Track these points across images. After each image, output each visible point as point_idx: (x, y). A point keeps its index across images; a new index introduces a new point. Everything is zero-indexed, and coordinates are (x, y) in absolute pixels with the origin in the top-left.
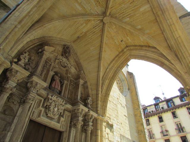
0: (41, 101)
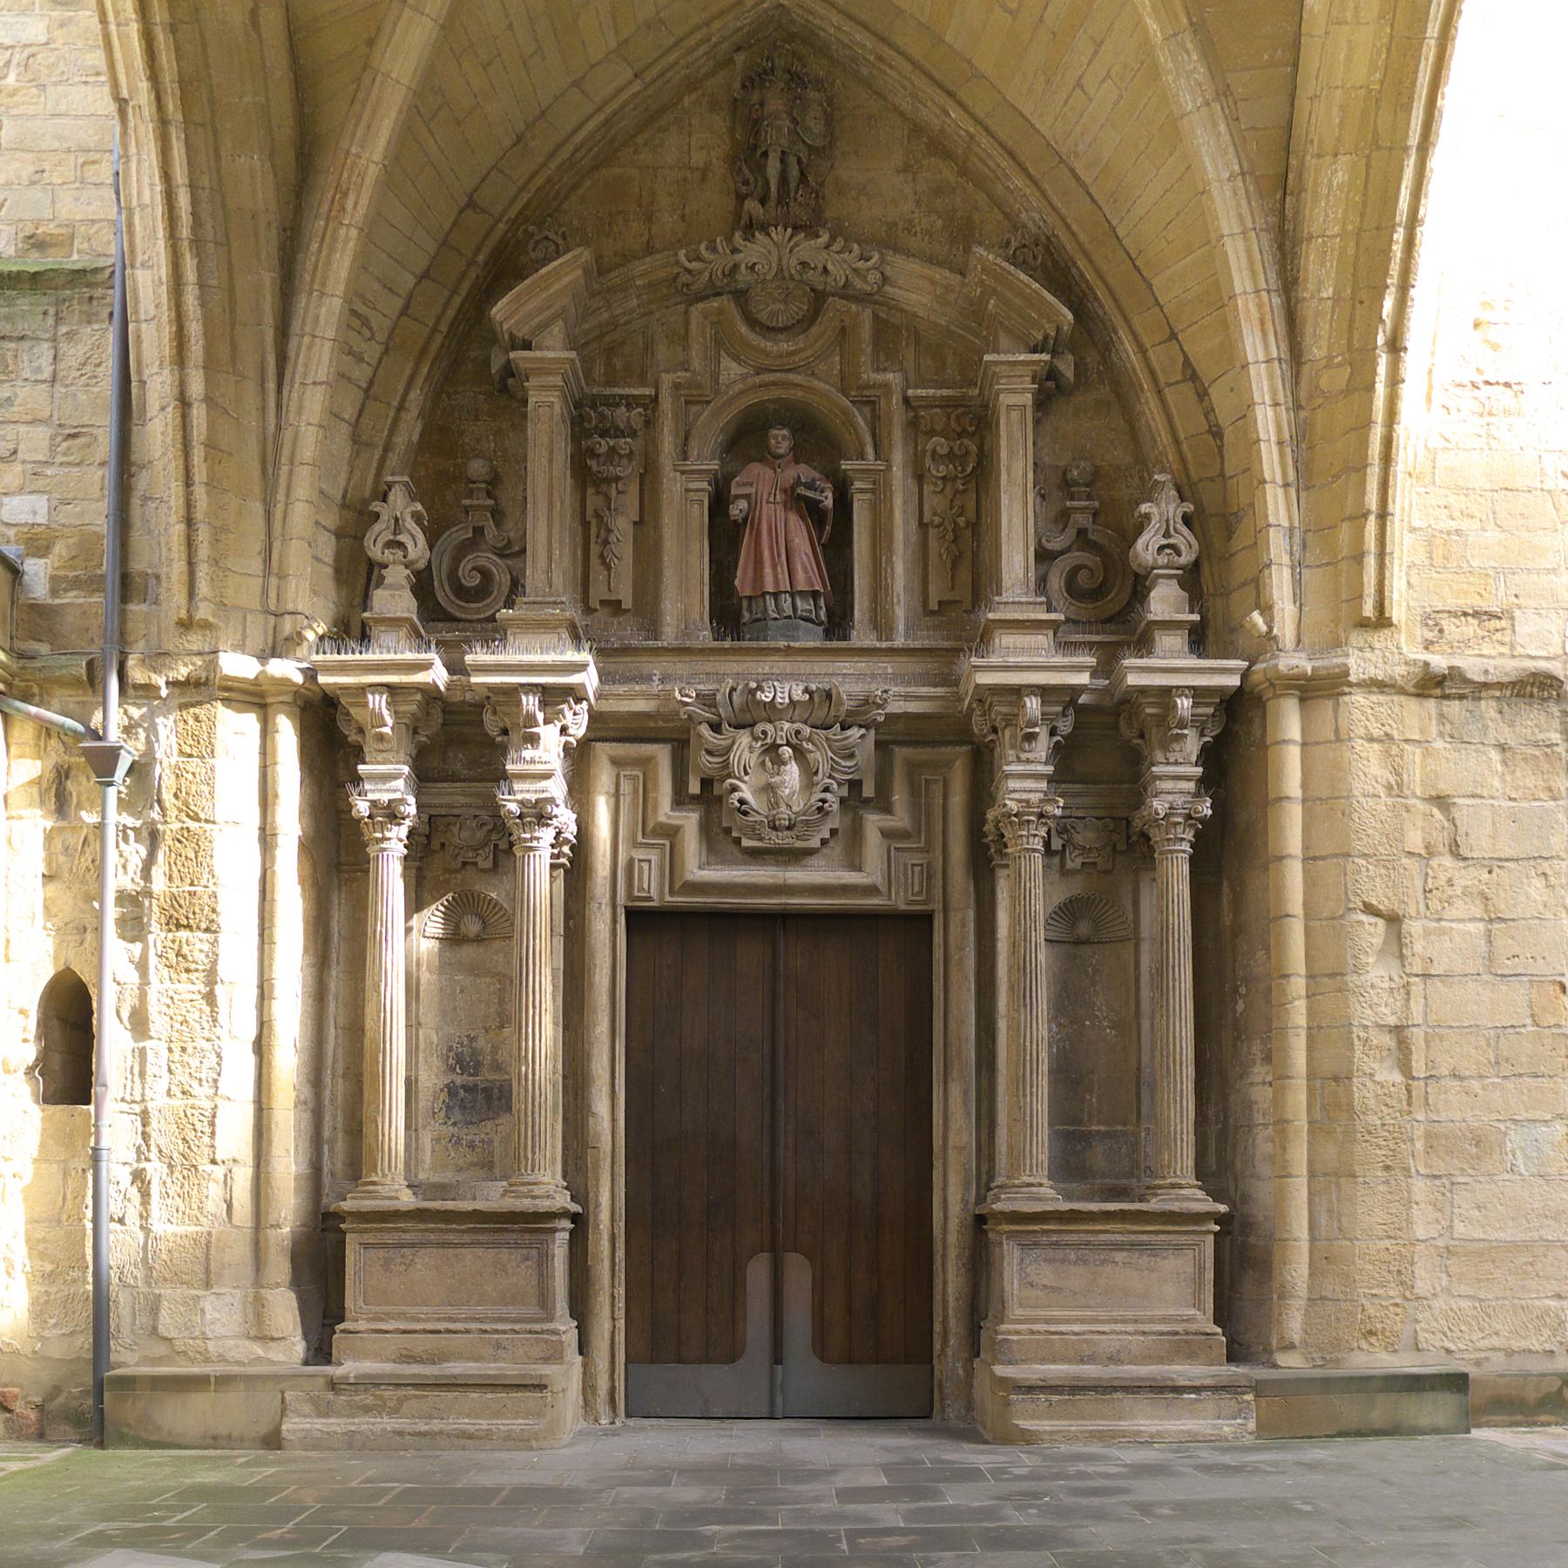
0: (645, 763)
